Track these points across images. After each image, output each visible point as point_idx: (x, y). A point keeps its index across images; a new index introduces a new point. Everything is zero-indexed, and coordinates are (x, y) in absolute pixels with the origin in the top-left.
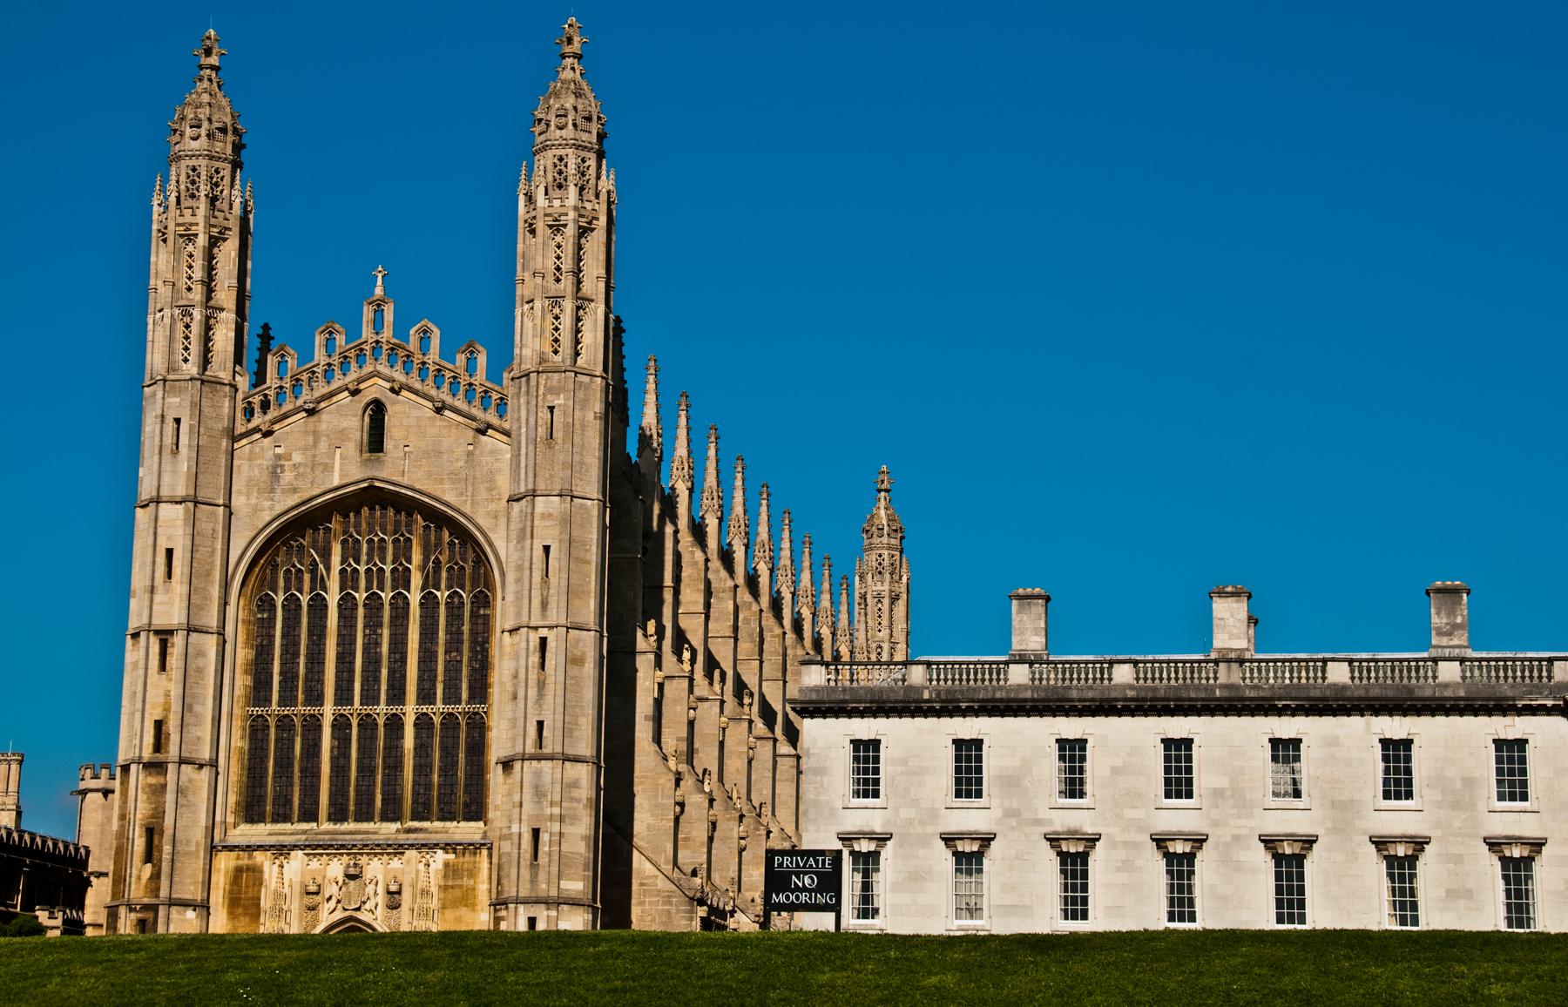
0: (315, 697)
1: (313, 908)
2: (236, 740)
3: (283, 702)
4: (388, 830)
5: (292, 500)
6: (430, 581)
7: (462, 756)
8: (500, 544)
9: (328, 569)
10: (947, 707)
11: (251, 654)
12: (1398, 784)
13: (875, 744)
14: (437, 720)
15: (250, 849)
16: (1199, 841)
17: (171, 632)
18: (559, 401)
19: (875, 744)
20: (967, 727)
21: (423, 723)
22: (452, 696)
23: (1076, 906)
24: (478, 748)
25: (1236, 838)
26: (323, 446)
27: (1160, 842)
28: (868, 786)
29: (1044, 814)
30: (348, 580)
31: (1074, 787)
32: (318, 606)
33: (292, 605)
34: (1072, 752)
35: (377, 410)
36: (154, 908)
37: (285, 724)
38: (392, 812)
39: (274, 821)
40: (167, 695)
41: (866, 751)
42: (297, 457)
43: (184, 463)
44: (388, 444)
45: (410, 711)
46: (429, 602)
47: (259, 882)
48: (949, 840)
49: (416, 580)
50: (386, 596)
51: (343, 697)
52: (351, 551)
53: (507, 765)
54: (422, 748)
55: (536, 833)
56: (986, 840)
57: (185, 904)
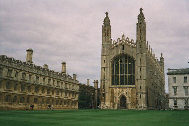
0: (118, 74)
1: (119, 93)
2: (111, 77)
3: (115, 74)
4: (126, 86)
5: (115, 55)
6: (129, 62)
11: (112, 70)
13: (176, 77)
14: (130, 76)
15: (113, 88)
17: (105, 68)
18: (141, 44)
19: (176, 77)
21: (128, 76)
24: (134, 78)
26: (118, 49)
28: (175, 81)
30: (121, 62)
32: (118, 65)
35: (123, 46)
36: (104, 93)
39: (115, 85)
40: (105, 73)
41: (175, 78)
43: (105, 52)
44: (125, 49)
45: (127, 75)
46: (129, 64)
47: (114, 91)
48: (184, 87)
49: (127, 62)
50: (125, 64)
51: (121, 73)
52: (121, 60)
53: (137, 80)
54: (129, 78)
55: (140, 86)
57: (107, 93)
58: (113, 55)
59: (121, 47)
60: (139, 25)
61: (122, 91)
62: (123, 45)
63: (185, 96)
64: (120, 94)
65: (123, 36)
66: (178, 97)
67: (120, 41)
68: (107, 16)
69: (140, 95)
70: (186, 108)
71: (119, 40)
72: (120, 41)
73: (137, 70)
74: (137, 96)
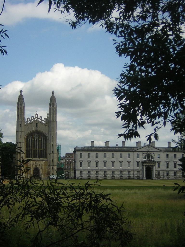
0: (32, 148)
3: (29, 148)
7: (44, 153)
8: (48, 136)
9: (32, 137)
10: (88, 151)
12: (121, 157)
14: (42, 150)
16: (107, 161)
20: (89, 152)
21: (41, 150)
22: (43, 148)
23: (97, 166)
25: (109, 161)
26: (32, 127)
27: (104, 161)
28: (81, 157)
29: (95, 159)
31: (97, 157)
32: (32, 140)
33: (29, 140)
34: (97, 154)
35: (37, 124)
37: (29, 150)
38: (39, 158)
42: (30, 127)
46: (41, 140)
48: (88, 161)
49: (40, 138)
51: (34, 148)
53: (50, 154)
56: (91, 161)
58: (28, 132)
59: (35, 125)
60: (52, 107)
61: (36, 163)
62: (36, 123)
63: (88, 168)
64: (34, 166)
65: (37, 114)
66: (83, 169)
67: (34, 119)
68: (21, 94)
69: (52, 167)
70: (89, 178)
71: (33, 118)
72: (34, 119)
73: (49, 146)
74: (48, 167)
